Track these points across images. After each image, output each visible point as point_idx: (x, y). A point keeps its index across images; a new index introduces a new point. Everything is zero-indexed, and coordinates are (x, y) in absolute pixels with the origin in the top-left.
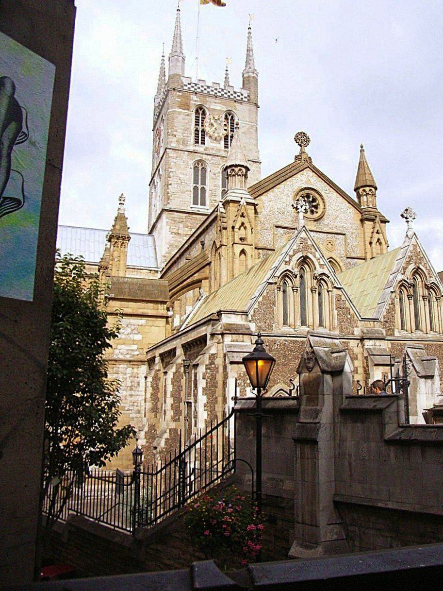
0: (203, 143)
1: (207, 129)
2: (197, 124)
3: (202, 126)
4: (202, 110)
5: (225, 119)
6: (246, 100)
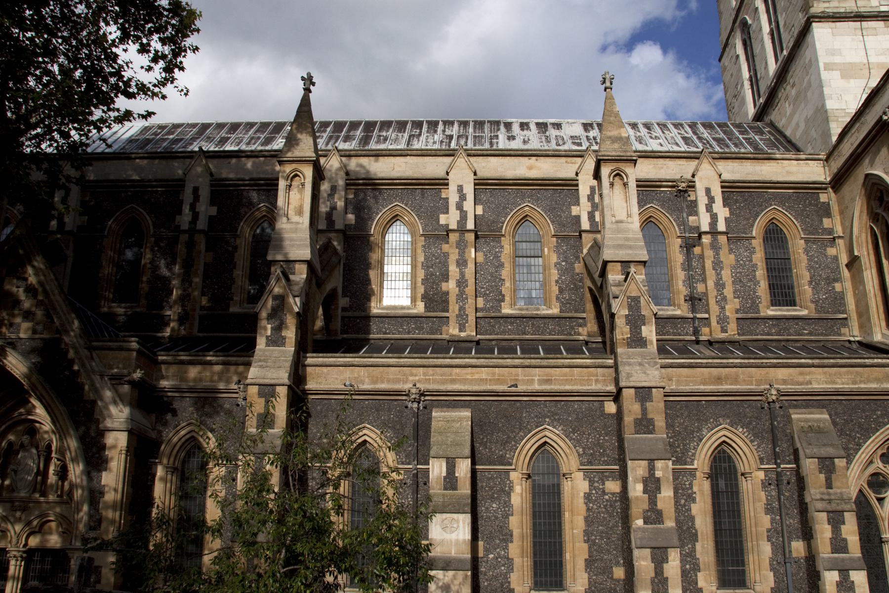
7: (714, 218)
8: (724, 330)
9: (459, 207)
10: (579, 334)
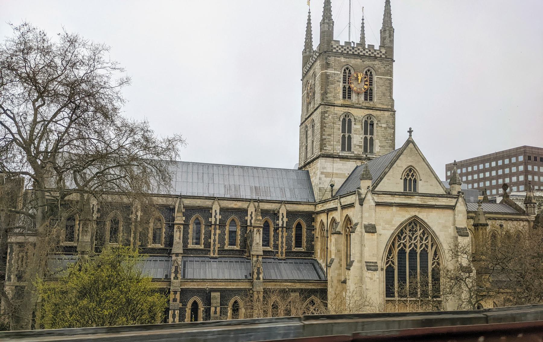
1: (352, 86)
3: (348, 83)
4: (348, 70)
7: (283, 222)
8: (282, 256)
9: (215, 217)
10: (244, 255)
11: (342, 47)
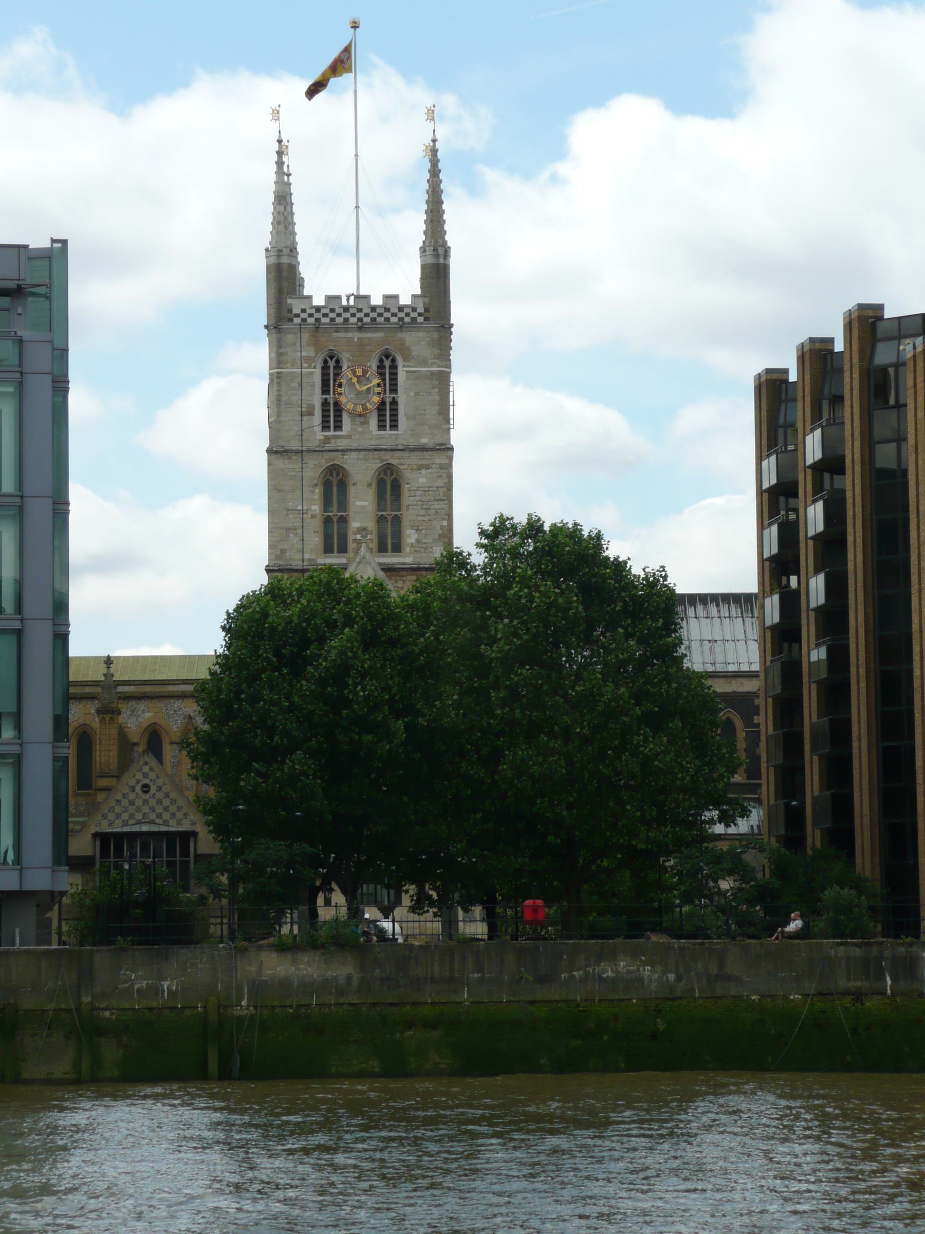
0: (338, 427)
1: (343, 399)
2: (325, 390)
3: (334, 394)
5: (379, 367)
6: (420, 319)
11: (318, 309)
